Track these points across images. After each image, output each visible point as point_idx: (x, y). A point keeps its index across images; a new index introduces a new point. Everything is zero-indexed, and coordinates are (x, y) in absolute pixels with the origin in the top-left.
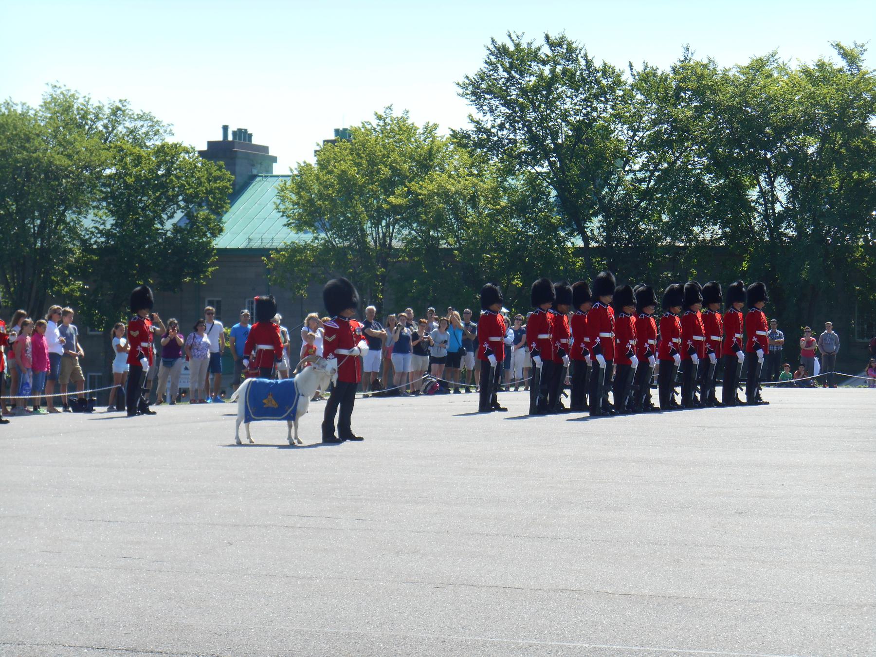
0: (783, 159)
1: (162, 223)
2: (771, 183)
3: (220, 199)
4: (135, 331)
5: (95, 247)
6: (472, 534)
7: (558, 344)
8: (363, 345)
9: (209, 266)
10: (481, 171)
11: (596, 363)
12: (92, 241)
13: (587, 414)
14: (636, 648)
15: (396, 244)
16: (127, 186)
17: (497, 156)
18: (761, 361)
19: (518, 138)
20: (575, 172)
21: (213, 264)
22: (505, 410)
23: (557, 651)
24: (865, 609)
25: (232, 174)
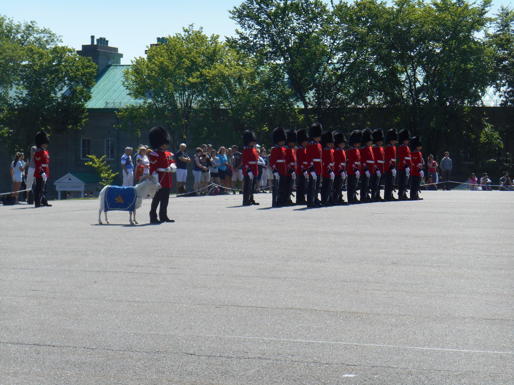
0: (421, 56)
1: (55, 93)
2: (414, 70)
3: (90, 79)
4: (38, 157)
5: (16, 107)
6: (238, 276)
7: (289, 166)
8: (173, 165)
9: (83, 118)
10: (244, 63)
11: (311, 177)
12: (15, 104)
13: (306, 206)
14: (333, 342)
15: (194, 106)
16: (35, 71)
17: (253, 54)
18: (408, 175)
19: (266, 43)
20: (298, 64)
21: (86, 117)
22: (258, 204)
23: (287, 344)
25: (96, 64)
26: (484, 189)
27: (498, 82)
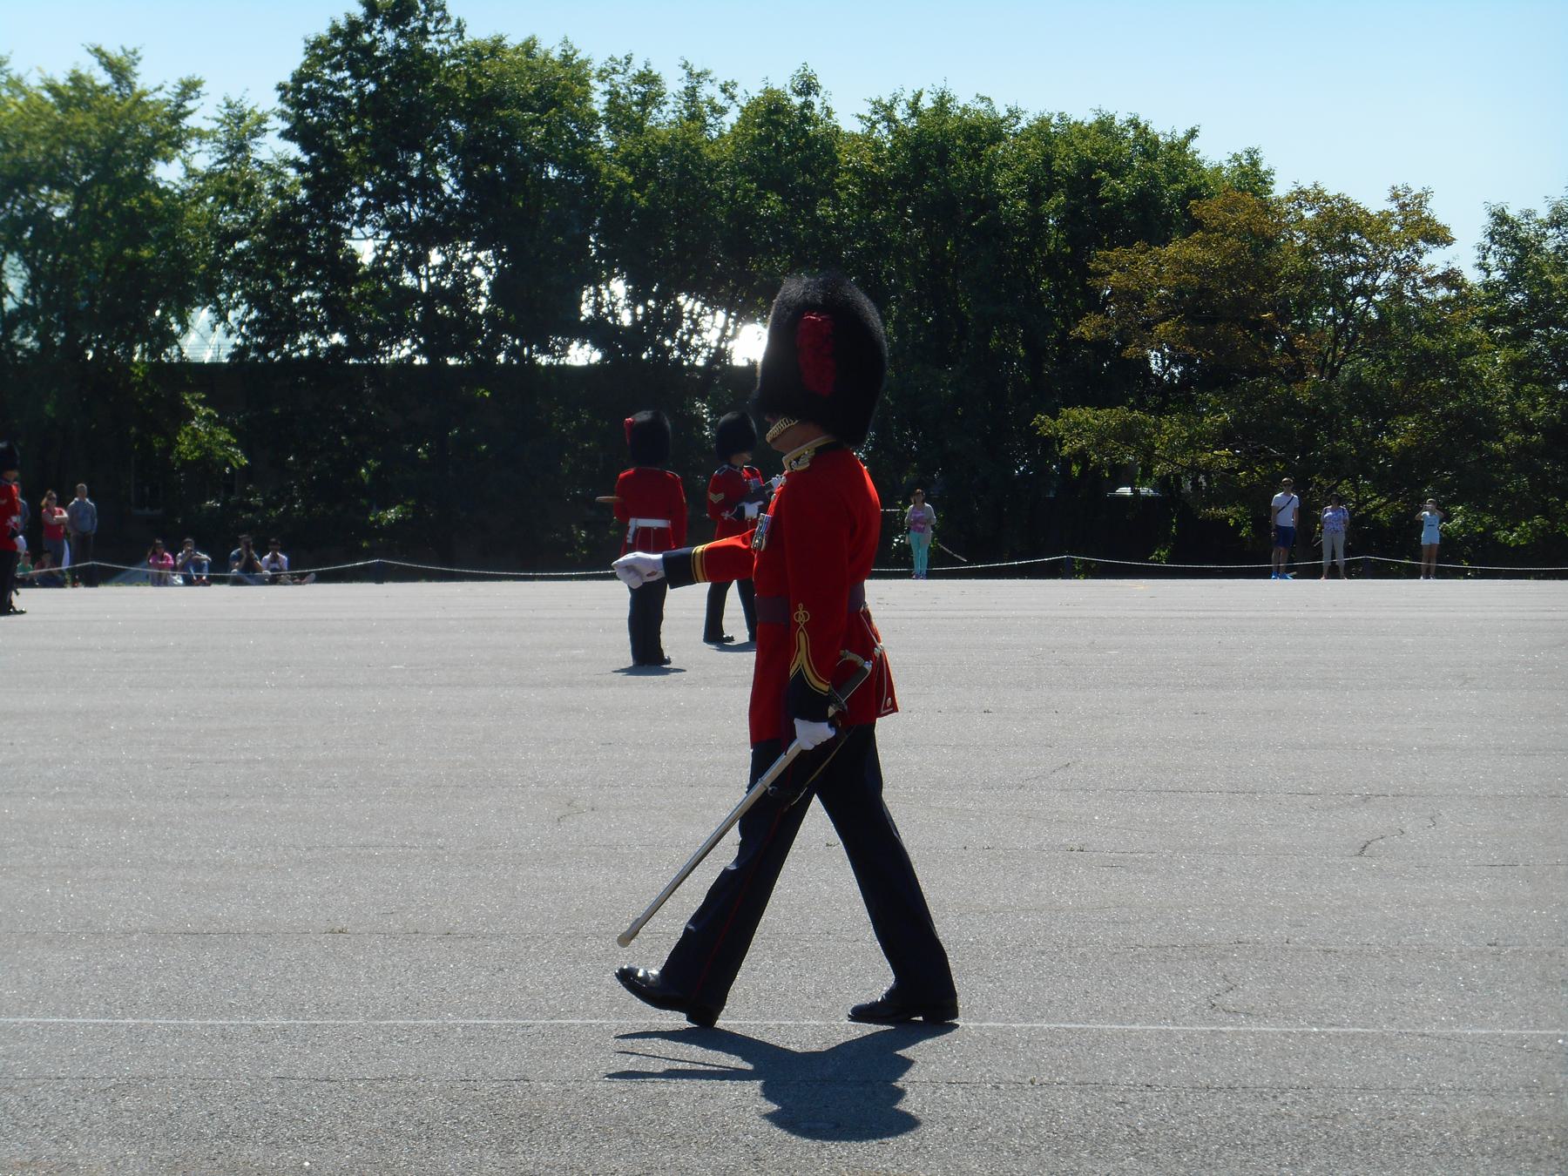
24: (135, 938)
26: (189, 582)
27: (222, 296)
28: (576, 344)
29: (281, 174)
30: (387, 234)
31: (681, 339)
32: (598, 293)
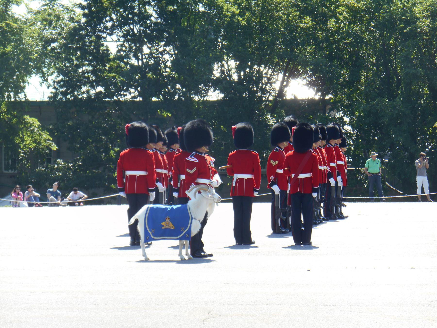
26: (30, 205)
28: (212, 90)
29: (72, 11)
30: (122, 39)
31: (262, 87)
32: (222, 66)
